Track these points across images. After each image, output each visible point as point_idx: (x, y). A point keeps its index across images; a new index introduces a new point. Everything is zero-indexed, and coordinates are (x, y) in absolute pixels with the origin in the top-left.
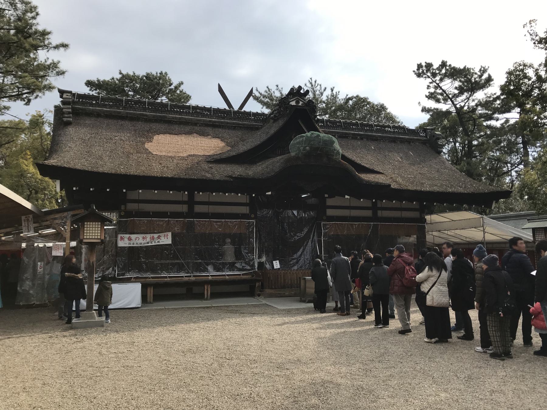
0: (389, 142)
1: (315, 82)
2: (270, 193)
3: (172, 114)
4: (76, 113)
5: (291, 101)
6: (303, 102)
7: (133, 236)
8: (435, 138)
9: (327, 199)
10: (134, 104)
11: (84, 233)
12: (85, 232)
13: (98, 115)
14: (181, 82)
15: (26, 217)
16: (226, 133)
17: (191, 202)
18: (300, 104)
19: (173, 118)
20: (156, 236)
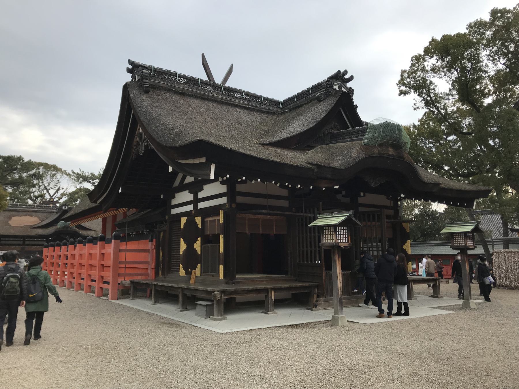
18: (66, 208)
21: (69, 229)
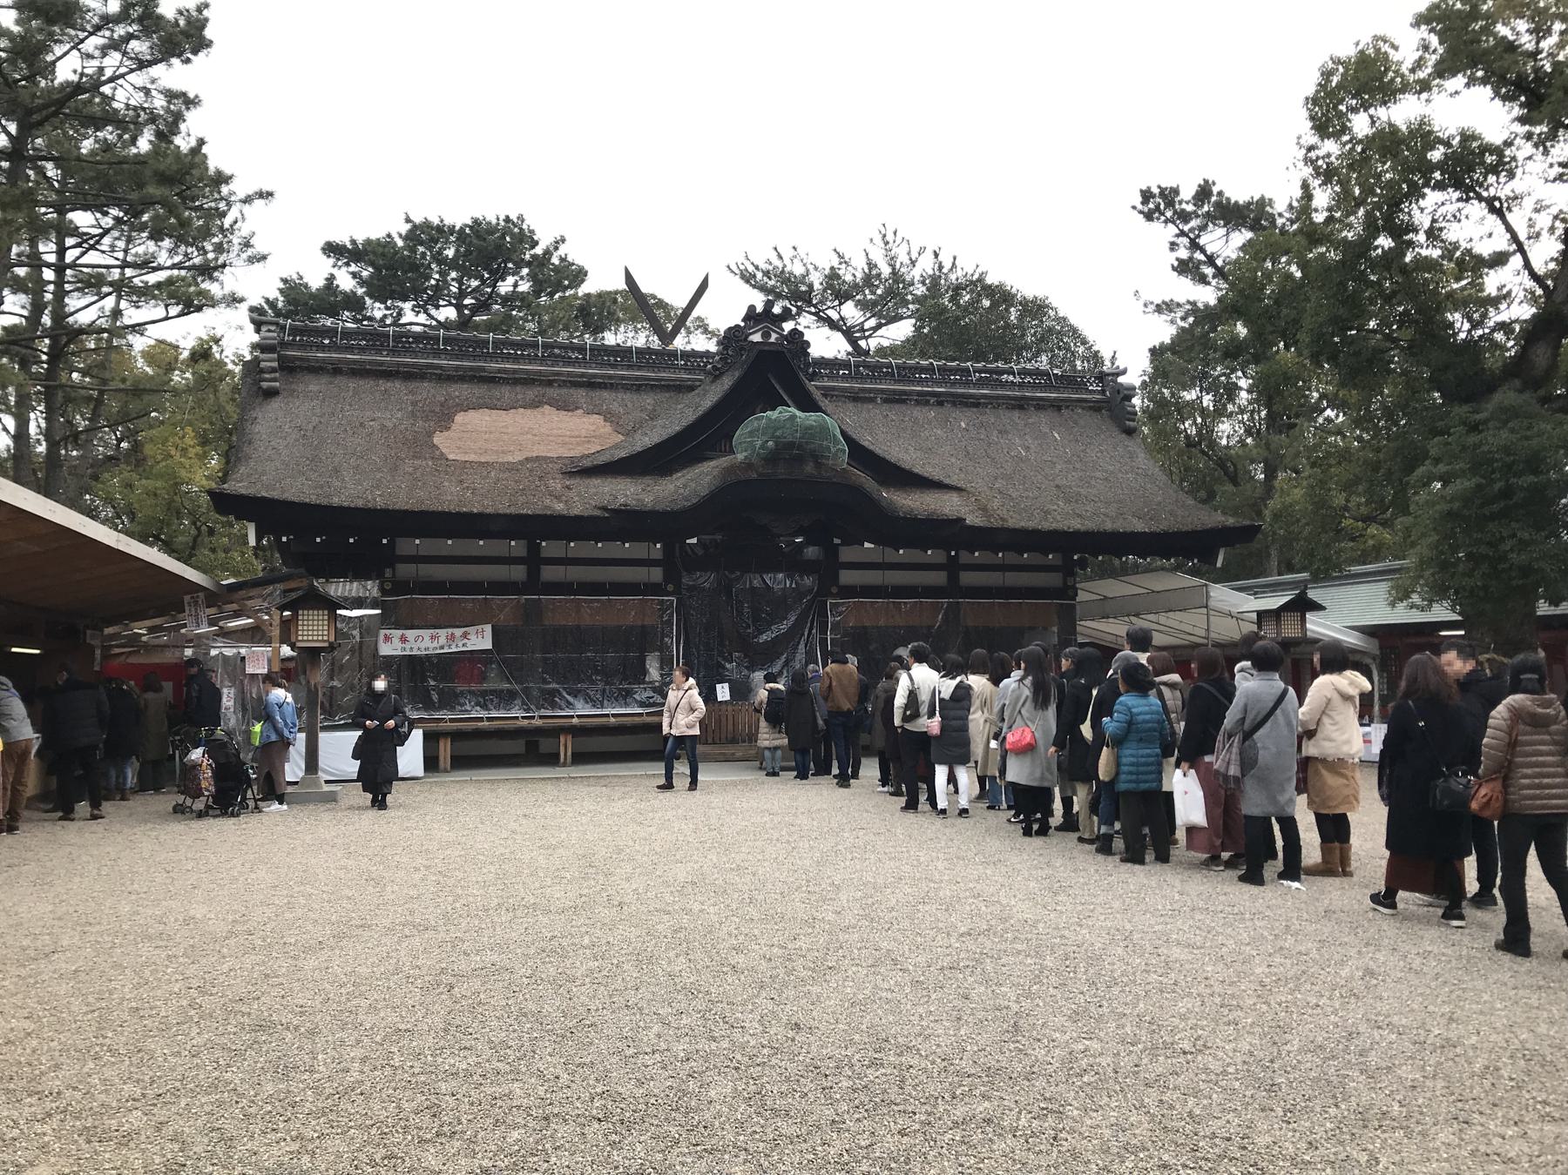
0: (1007, 408)
1: (895, 233)
2: (694, 541)
3: (497, 362)
4: (289, 368)
5: (751, 334)
6: (778, 333)
7: (411, 634)
8: (1122, 395)
9: (841, 548)
10: (413, 342)
11: (297, 630)
12: (300, 628)
13: (336, 370)
14: (559, 238)
15: (192, 598)
16: (614, 401)
19: (500, 370)
20: (458, 632)
21: (809, 468)
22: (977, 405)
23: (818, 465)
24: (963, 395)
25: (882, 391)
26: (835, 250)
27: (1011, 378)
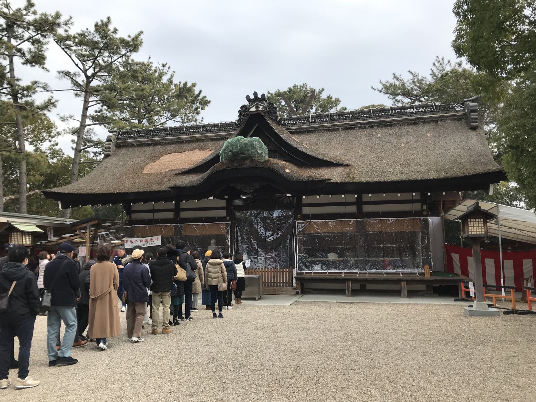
0: (408, 125)
1: (443, 59)
4: (118, 146)
5: (251, 108)
6: (262, 106)
7: (134, 240)
14: (321, 89)
17: (177, 210)
18: (261, 108)
20: (149, 239)
21: (248, 162)
22: (391, 125)
23: (252, 160)
24: (384, 122)
25: (343, 125)
26: (409, 72)
27: (412, 110)
